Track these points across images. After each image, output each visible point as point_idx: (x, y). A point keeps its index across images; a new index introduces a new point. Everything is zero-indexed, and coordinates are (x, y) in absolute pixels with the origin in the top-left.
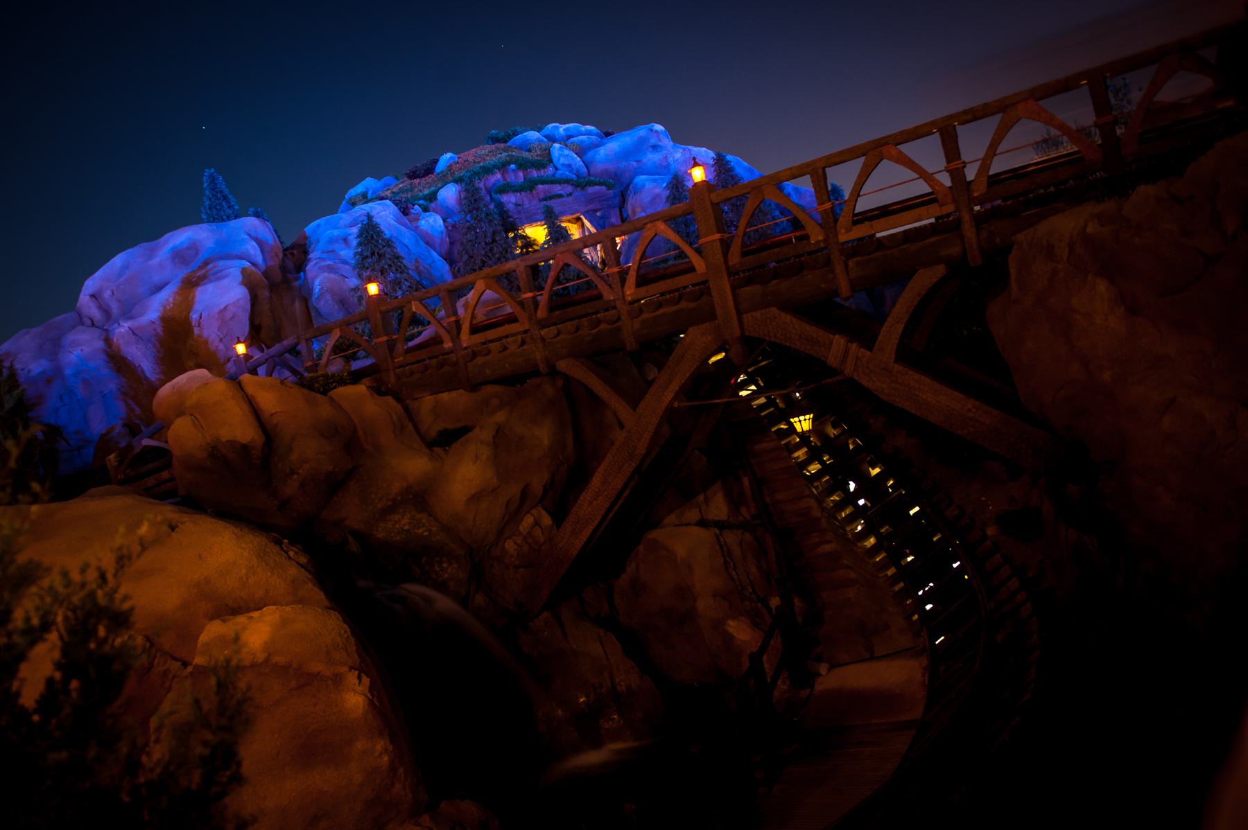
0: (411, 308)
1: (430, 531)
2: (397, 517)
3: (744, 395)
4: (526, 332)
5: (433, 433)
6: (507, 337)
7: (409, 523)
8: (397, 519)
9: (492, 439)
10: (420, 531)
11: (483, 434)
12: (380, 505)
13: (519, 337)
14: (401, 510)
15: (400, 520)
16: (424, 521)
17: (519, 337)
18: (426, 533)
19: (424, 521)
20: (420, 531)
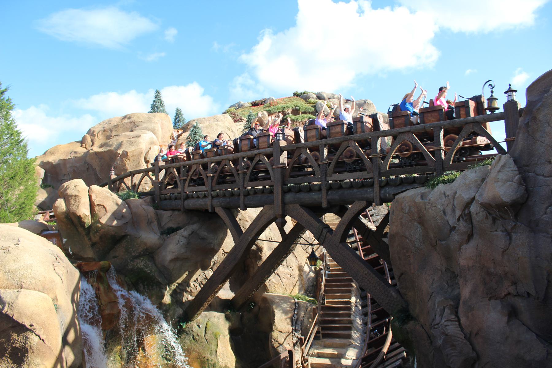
0: (170, 171)
1: (151, 271)
2: (139, 261)
3: (233, 244)
4: (207, 191)
5: (166, 227)
6: (199, 191)
7: (143, 265)
8: (139, 262)
9: (188, 236)
10: (147, 270)
11: (184, 232)
12: (133, 254)
13: (203, 193)
14: (142, 258)
15: (140, 262)
16: (150, 265)
17: (203, 193)
18: (149, 271)
19: (150, 265)
20: (147, 269)
